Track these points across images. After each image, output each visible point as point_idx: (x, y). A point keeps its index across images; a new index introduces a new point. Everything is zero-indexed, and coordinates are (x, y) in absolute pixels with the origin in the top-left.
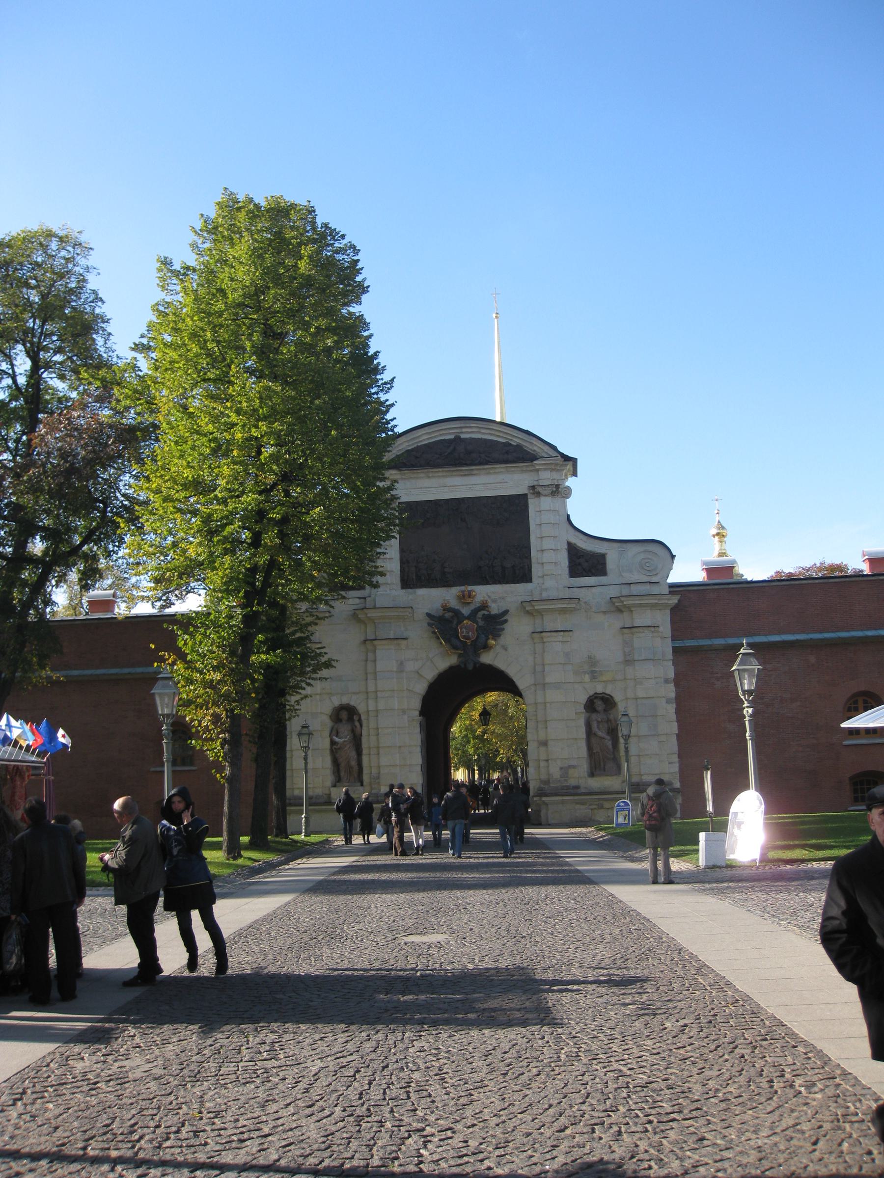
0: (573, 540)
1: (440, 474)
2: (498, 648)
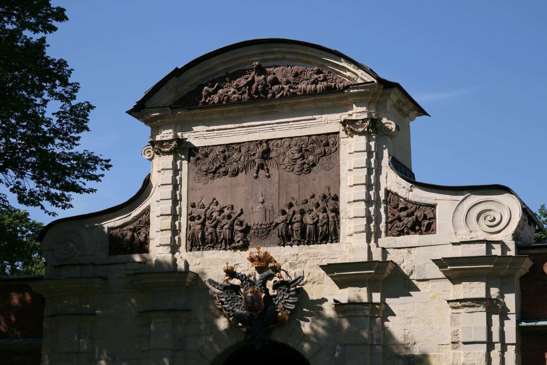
0: (394, 189)
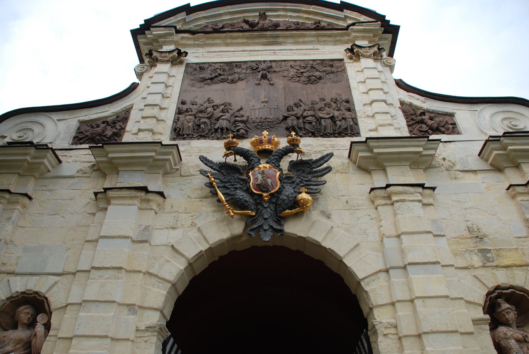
1: (240, 41)
2: (315, 215)
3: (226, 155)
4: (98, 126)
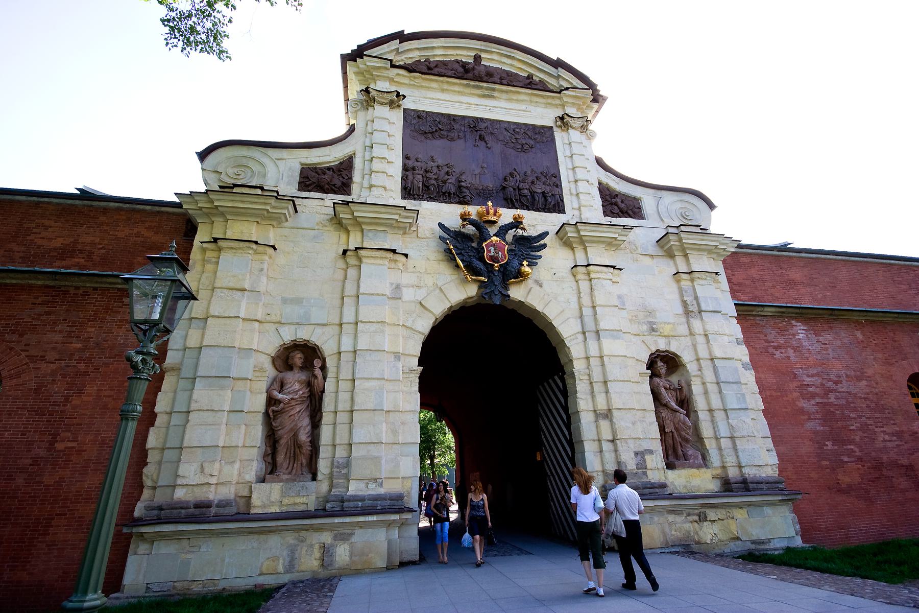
1: (456, 88)
2: (530, 282)
3: (464, 226)
4: (324, 174)
